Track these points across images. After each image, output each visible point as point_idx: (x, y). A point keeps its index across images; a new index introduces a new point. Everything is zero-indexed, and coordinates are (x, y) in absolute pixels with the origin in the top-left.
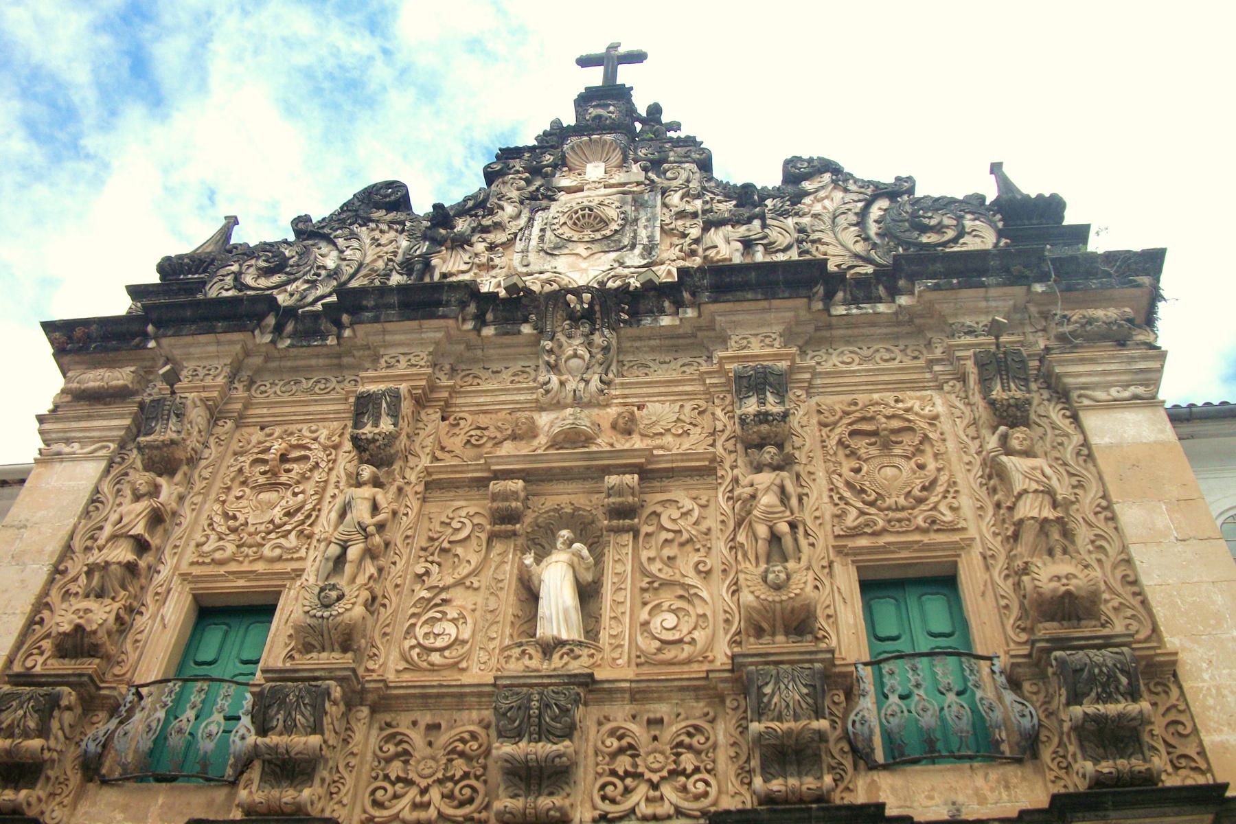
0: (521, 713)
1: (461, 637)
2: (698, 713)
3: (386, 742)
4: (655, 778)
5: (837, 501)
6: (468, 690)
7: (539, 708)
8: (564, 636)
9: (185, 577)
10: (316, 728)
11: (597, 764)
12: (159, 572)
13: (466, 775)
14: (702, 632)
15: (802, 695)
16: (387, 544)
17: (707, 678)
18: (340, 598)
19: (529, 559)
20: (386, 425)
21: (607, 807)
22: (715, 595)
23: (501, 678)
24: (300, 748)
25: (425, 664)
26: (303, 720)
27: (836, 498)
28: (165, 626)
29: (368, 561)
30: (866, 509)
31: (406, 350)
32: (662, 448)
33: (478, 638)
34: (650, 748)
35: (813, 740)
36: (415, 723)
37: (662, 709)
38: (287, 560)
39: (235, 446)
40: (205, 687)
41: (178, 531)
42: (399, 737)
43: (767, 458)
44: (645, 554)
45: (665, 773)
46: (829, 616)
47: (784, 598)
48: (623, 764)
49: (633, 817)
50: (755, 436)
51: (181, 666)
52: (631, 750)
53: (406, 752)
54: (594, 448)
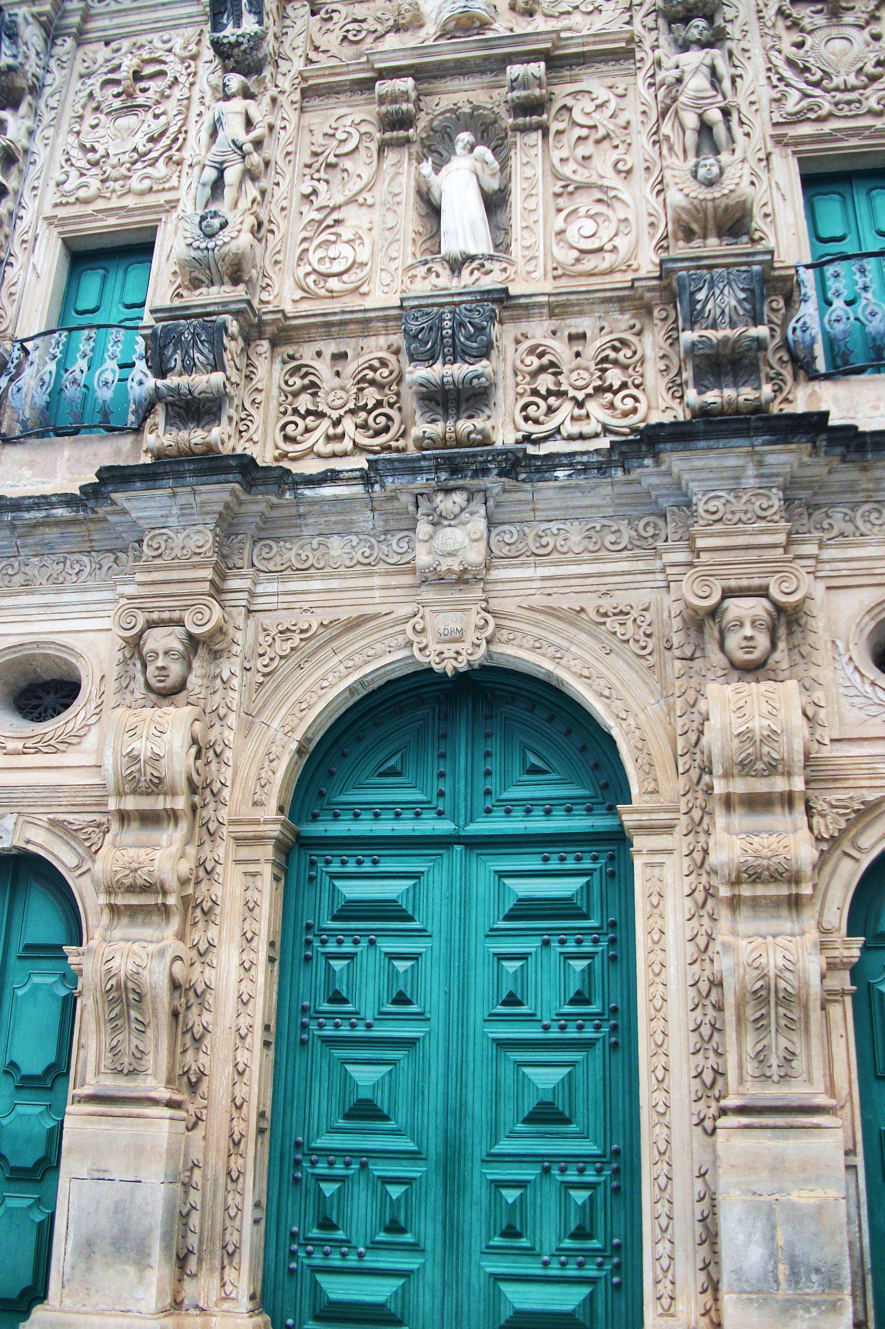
0: (433, 334)
1: (359, 260)
2: (623, 326)
3: (291, 376)
4: (580, 395)
5: (775, 82)
6: (372, 314)
7: (452, 328)
8: (472, 251)
9: (50, 220)
10: (217, 365)
11: (517, 385)
12: (21, 218)
13: (379, 404)
14: (626, 239)
15: (740, 302)
16: (267, 164)
17: (632, 287)
18: (224, 225)
19: (427, 168)
20: (249, 24)
21: (530, 427)
22: (637, 196)
23: (409, 299)
24: (202, 386)
25: (323, 292)
26: (202, 358)
27: (774, 78)
29: (249, 183)
30: (810, 90)
32: (570, 29)
33: (379, 258)
34: (573, 366)
35: (750, 349)
36: (319, 354)
37: (583, 324)
38: (158, 191)
39: (80, 68)
40: (93, 334)
41: (33, 171)
42: (304, 370)
43: (694, 33)
44: (556, 155)
45: (590, 390)
46: (766, 215)
47: (717, 195)
48: (545, 382)
49: (558, 437)
50: (680, 8)
51: (63, 316)
52: (553, 368)
53: (313, 384)
54: (490, 35)
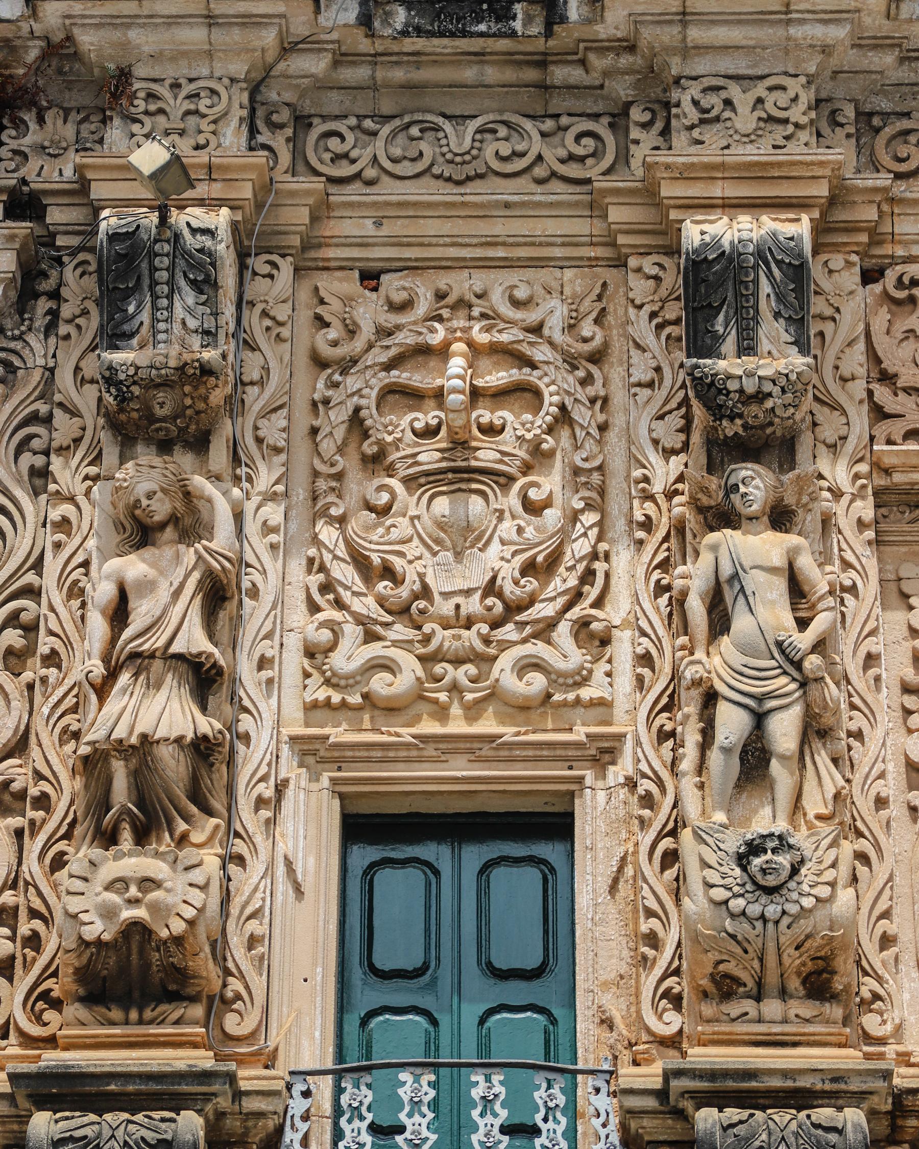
9: (309, 750)
28: (298, 891)
31: (741, 66)
38: (564, 704)
